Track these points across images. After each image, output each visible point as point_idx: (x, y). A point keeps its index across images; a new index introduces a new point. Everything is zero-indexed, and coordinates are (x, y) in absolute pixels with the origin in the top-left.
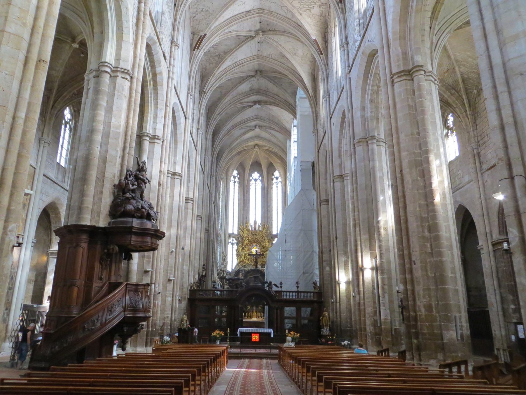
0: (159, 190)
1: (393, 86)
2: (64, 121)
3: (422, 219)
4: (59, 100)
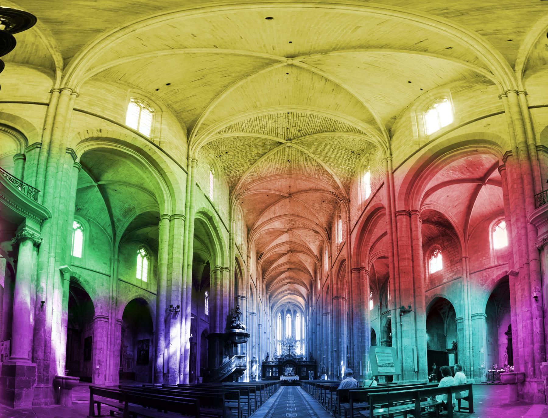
3: (359, 329)
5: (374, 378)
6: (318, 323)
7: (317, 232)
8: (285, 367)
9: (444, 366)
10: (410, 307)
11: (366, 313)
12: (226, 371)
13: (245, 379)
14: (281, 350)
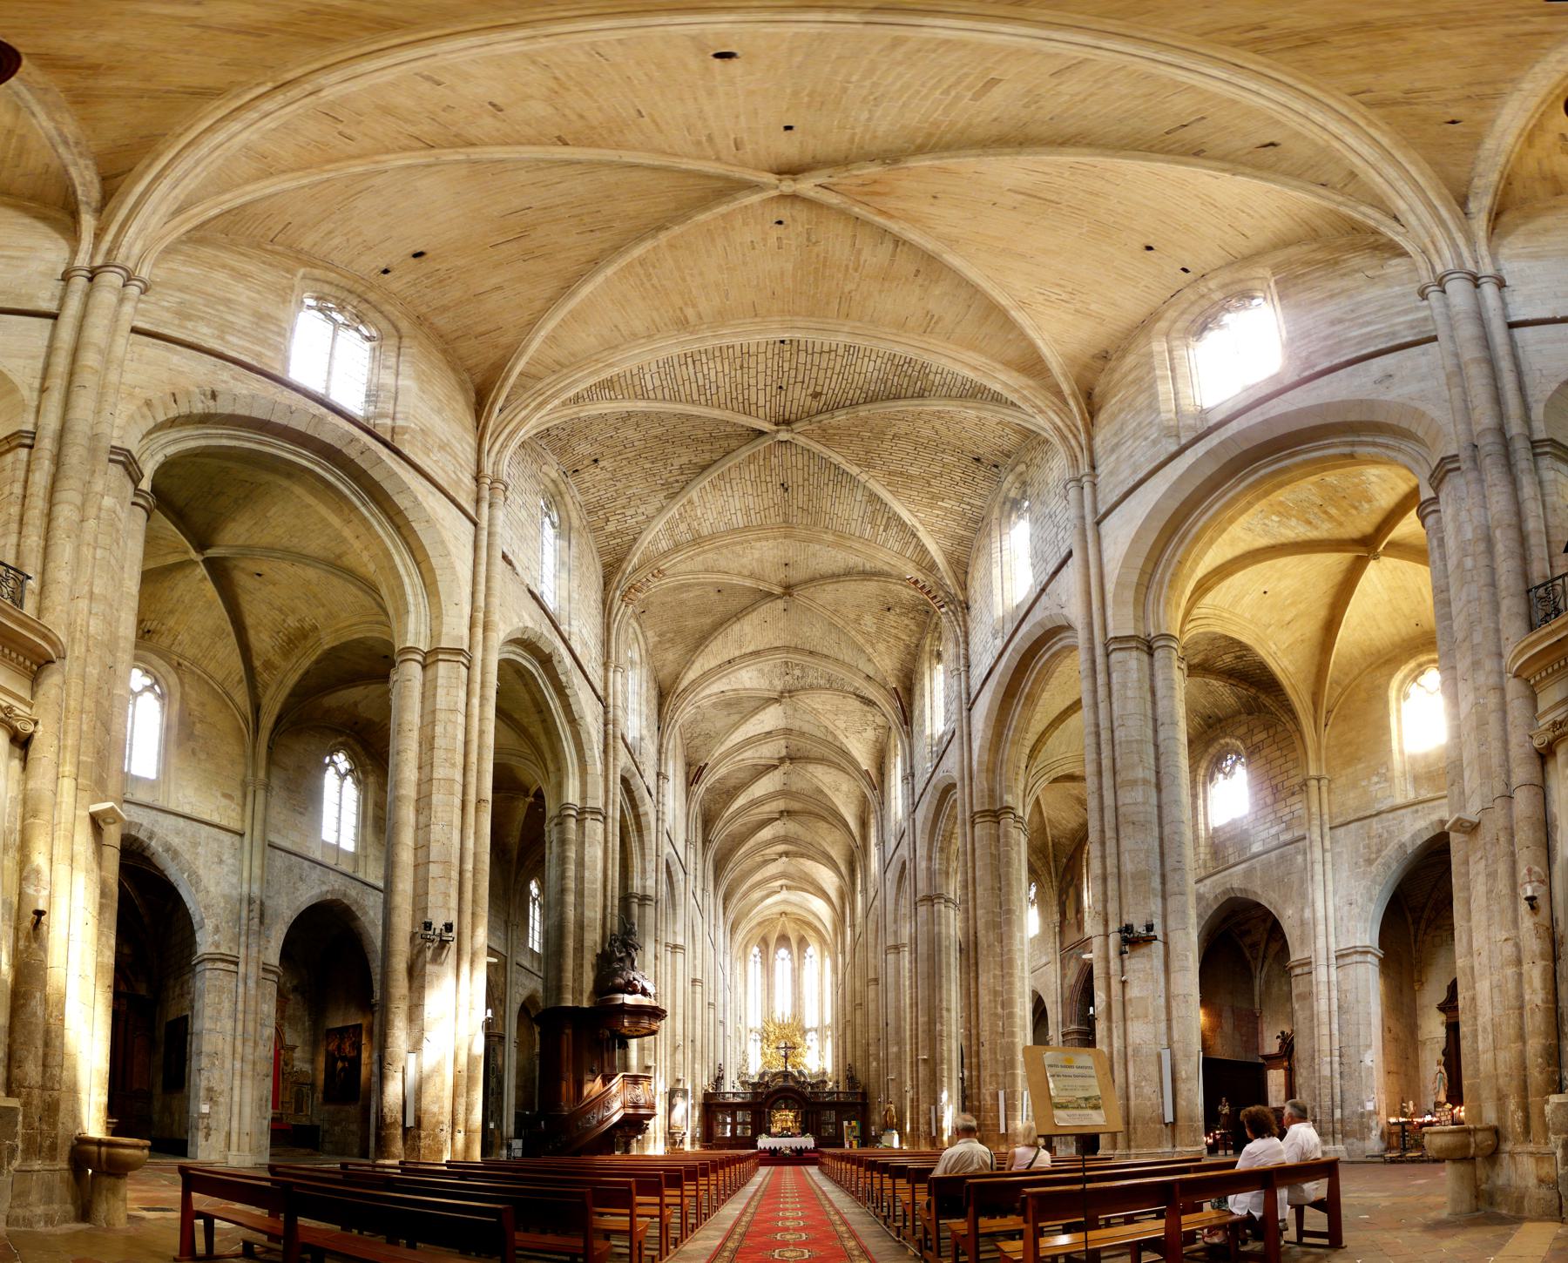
1: (973, 827)
5: (1041, 1141)
6: (872, 975)
7: (869, 702)
8: (771, 1108)
9: (1253, 1105)
10: (1150, 928)
11: (1017, 945)
12: (595, 1122)
13: (652, 1144)
14: (759, 1057)
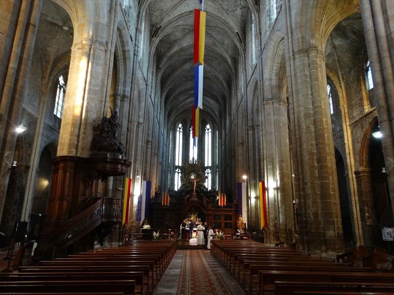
0: (127, 134)
2: (59, 86)
4: (55, 69)
